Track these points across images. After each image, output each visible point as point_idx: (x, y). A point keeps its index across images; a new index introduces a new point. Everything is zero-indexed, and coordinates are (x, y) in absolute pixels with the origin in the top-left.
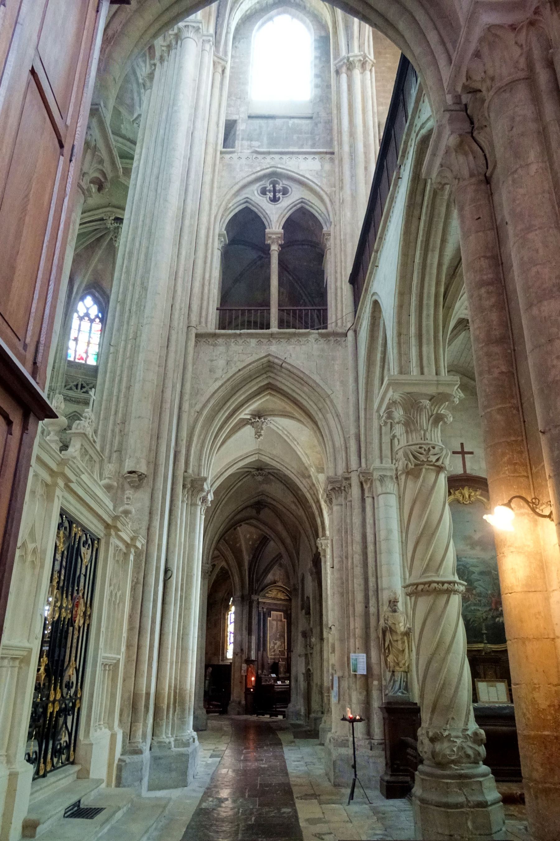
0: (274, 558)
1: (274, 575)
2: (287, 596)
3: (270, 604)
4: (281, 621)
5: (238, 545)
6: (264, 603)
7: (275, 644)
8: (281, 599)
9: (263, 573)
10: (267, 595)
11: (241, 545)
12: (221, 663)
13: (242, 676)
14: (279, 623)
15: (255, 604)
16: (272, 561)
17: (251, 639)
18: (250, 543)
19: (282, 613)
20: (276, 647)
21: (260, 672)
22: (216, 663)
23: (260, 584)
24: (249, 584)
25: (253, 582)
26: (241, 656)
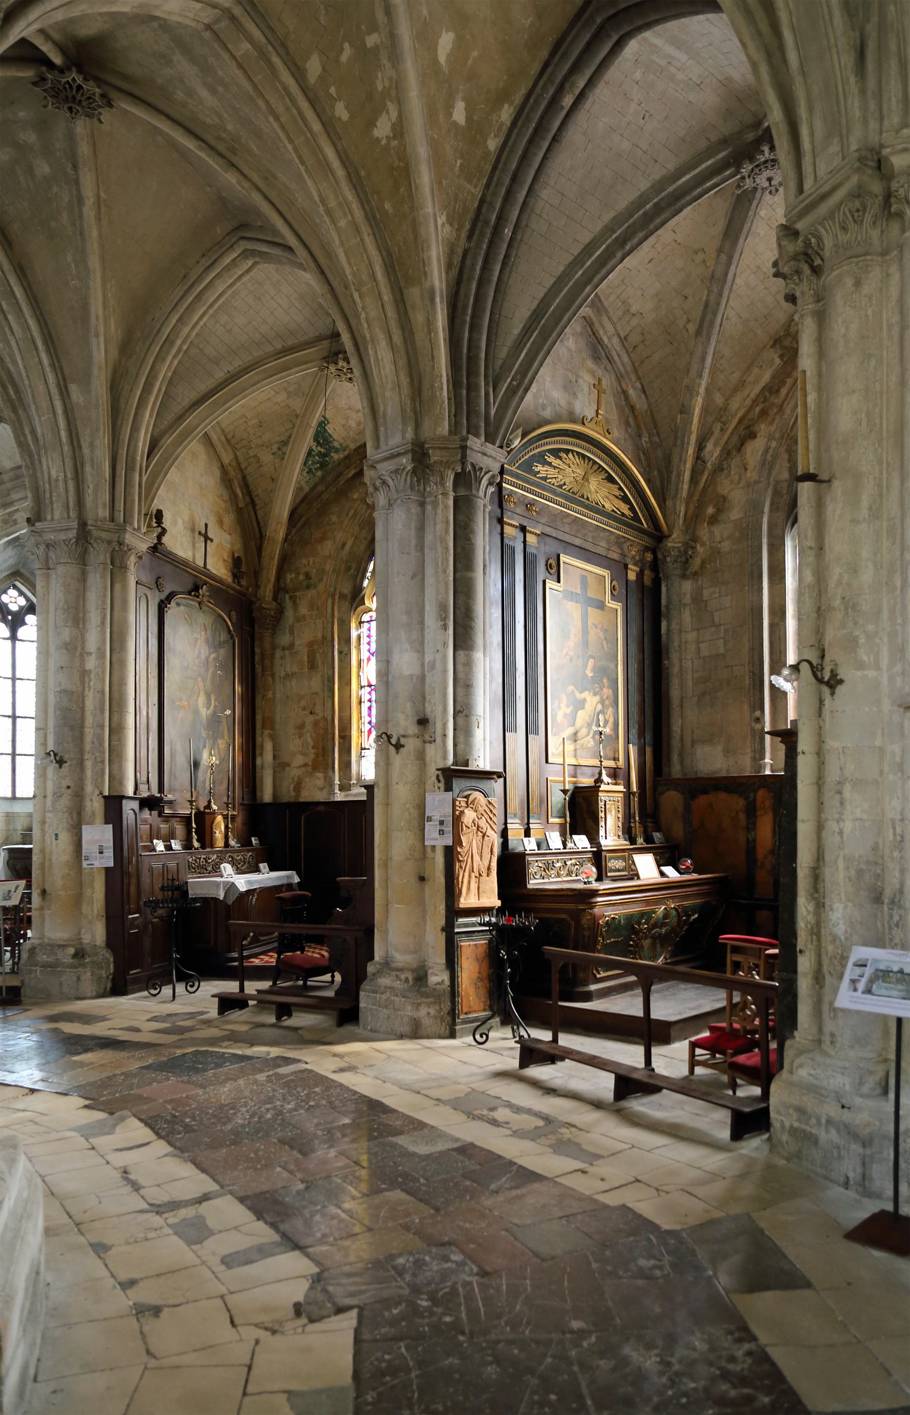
0: (588, 250)
1: (570, 387)
2: (625, 499)
3: (556, 518)
4: (601, 606)
5: (383, 129)
6: (529, 506)
7: (581, 705)
8: (598, 510)
9: (527, 330)
10: (539, 468)
11: (400, 129)
12: (339, 796)
13: (423, 852)
14: (594, 614)
15: (484, 494)
16: (578, 261)
17: (469, 664)
18: (459, 115)
19: (606, 573)
20: (583, 717)
21: (515, 828)
22: (321, 797)
23: (512, 391)
24: (455, 383)
25: (472, 372)
26: (421, 756)
